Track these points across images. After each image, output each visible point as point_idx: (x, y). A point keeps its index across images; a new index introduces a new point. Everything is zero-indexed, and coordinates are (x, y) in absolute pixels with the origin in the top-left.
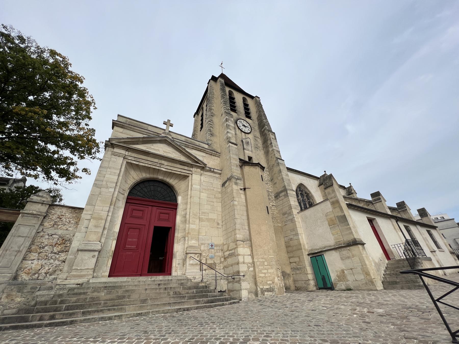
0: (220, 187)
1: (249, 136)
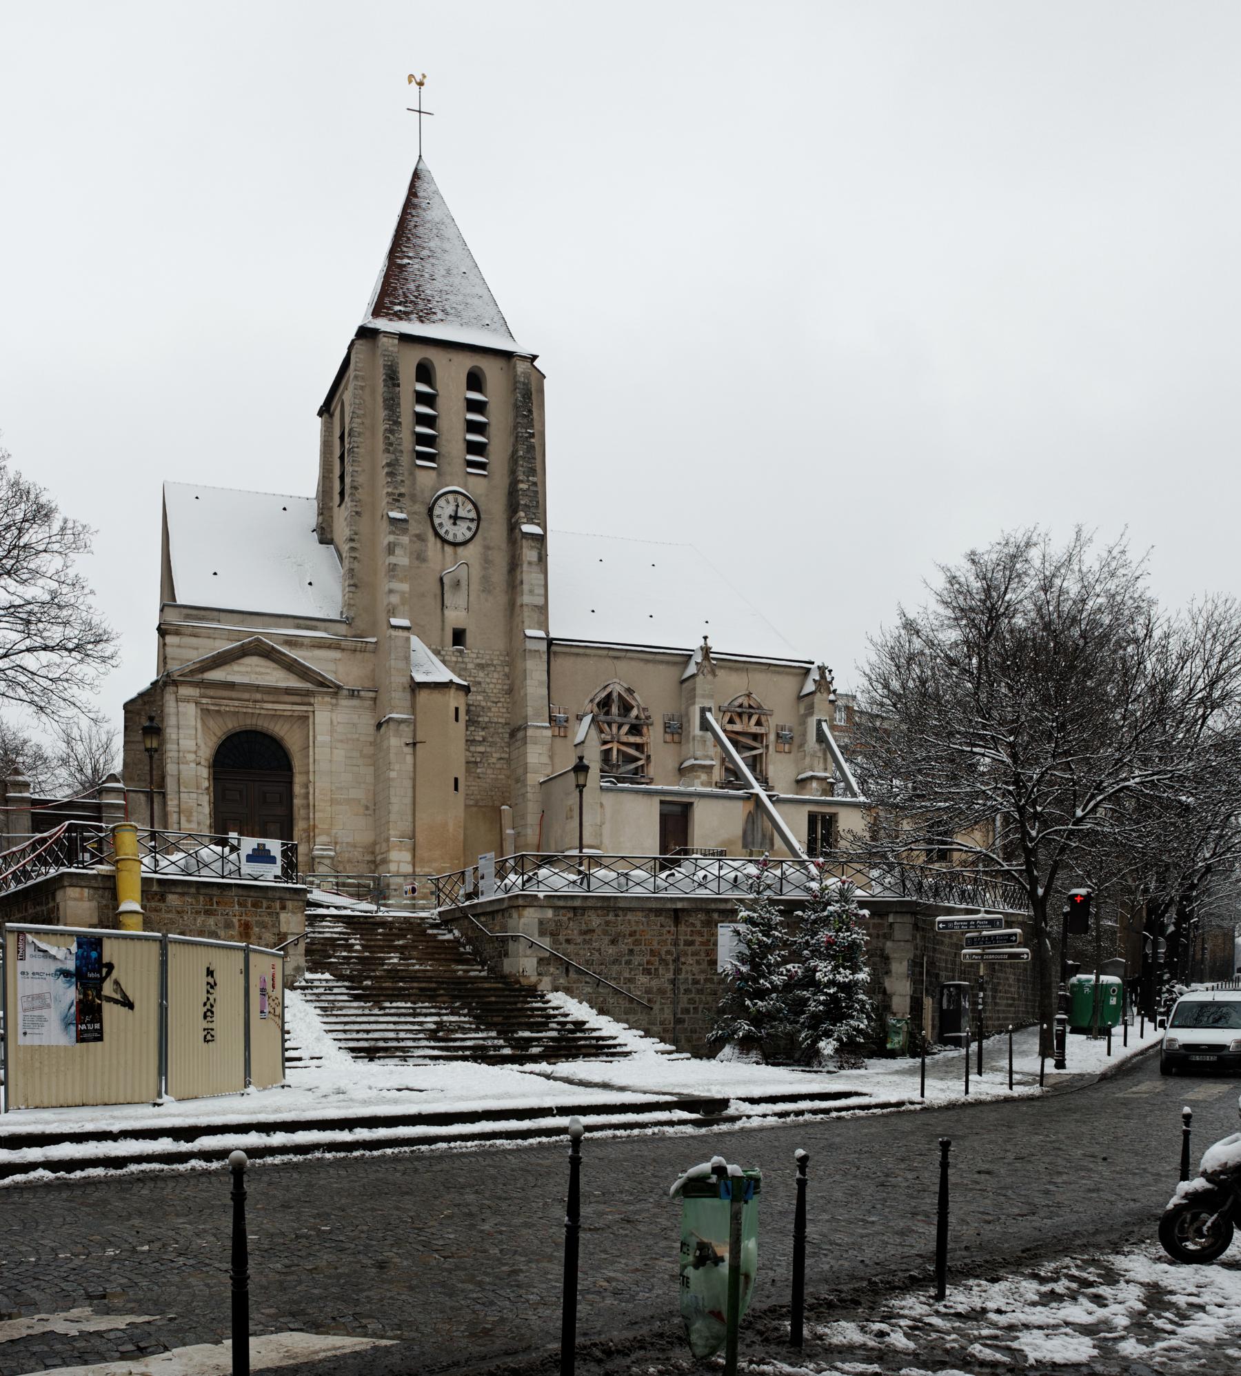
0: (372, 730)
1: (470, 553)
